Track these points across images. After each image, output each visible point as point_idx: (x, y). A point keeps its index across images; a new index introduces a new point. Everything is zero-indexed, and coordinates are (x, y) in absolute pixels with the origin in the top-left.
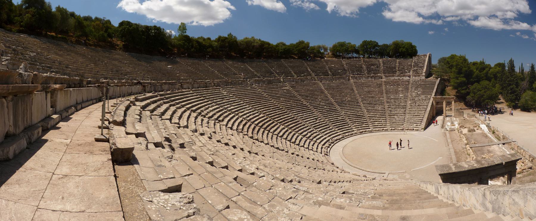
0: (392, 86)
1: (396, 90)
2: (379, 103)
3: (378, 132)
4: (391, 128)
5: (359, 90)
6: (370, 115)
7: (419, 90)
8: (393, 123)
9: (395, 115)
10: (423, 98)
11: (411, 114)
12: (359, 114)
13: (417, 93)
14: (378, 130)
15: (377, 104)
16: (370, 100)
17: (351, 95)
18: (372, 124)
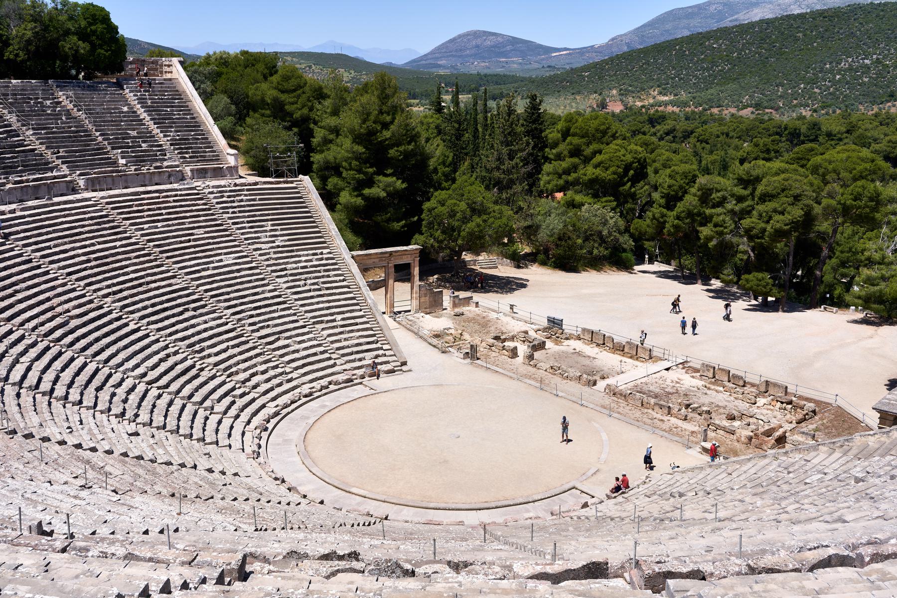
0: (158, 221)
1: (189, 241)
2: (188, 303)
3: (296, 408)
4: (317, 385)
5: (59, 261)
6: (209, 356)
7: (271, 230)
8: (304, 365)
9: (278, 339)
10: (311, 261)
11: (322, 322)
12: (176, 364)
13: (274, 242)
14: (293, 402)
15: (187, 310)
16: (149, 299)
17: (53, 288)
18: (255, 387)
